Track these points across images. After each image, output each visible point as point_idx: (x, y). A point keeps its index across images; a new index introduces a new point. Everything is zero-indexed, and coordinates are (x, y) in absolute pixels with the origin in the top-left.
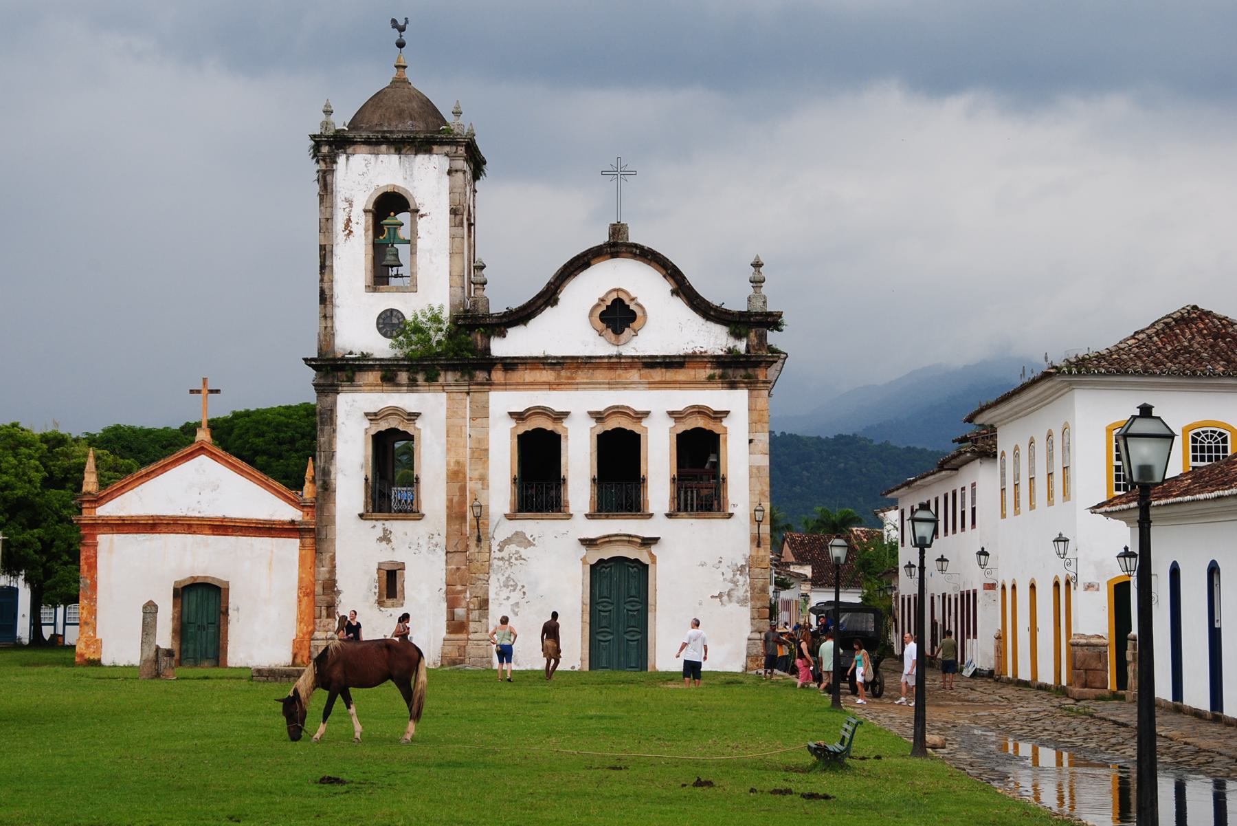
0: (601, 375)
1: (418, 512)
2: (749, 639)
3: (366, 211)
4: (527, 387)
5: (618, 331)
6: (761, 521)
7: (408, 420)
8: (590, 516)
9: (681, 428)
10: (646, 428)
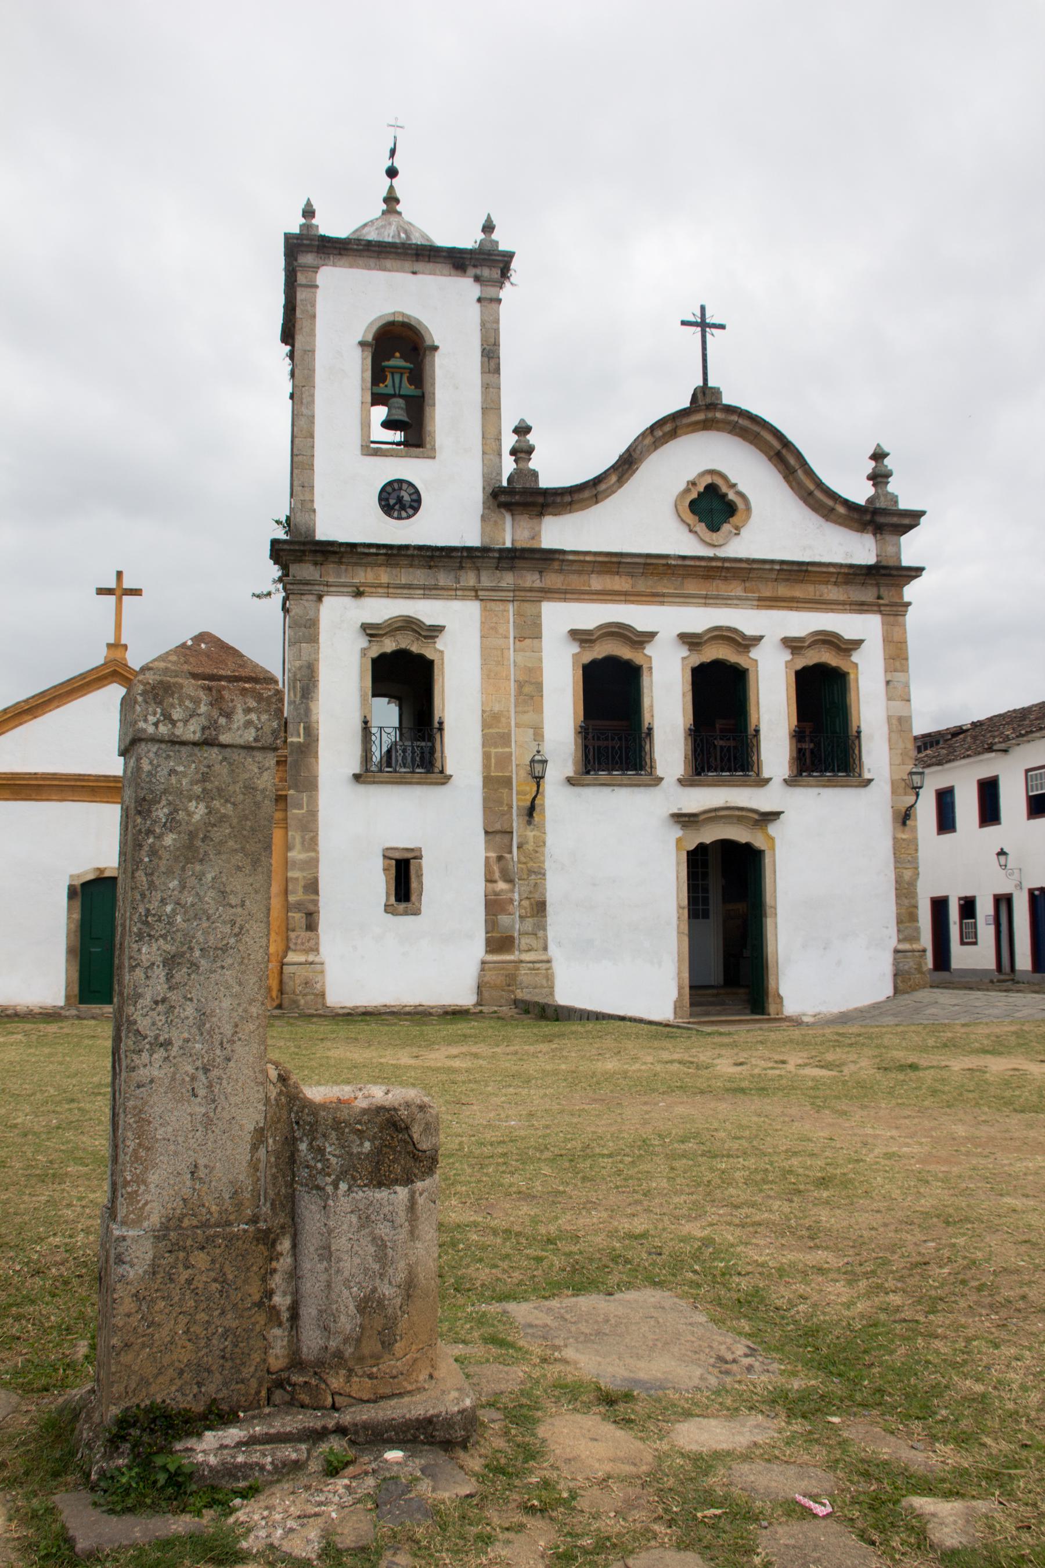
0: (692, 587)
1: (442, 772)
2: (897, 951)
3: (362, 344)
4: (595, 597)
5: (714, 528)
6: (920, 788)
7: (426, 637)
8: (681, 782)
9: (801, 663)
10: (756, 661)
